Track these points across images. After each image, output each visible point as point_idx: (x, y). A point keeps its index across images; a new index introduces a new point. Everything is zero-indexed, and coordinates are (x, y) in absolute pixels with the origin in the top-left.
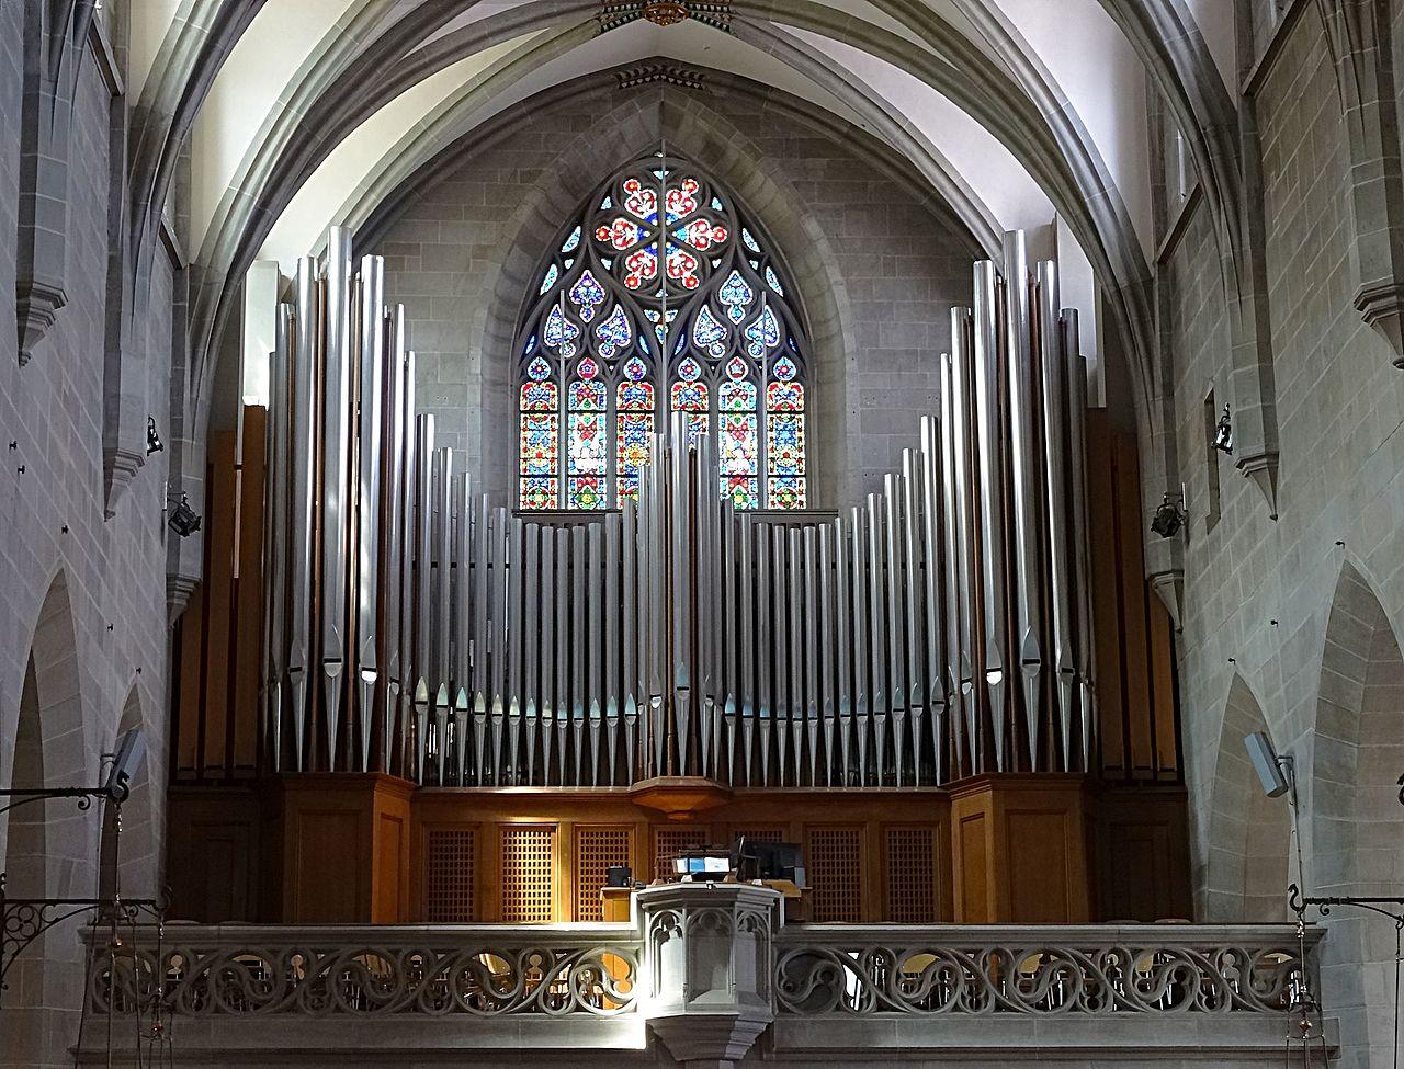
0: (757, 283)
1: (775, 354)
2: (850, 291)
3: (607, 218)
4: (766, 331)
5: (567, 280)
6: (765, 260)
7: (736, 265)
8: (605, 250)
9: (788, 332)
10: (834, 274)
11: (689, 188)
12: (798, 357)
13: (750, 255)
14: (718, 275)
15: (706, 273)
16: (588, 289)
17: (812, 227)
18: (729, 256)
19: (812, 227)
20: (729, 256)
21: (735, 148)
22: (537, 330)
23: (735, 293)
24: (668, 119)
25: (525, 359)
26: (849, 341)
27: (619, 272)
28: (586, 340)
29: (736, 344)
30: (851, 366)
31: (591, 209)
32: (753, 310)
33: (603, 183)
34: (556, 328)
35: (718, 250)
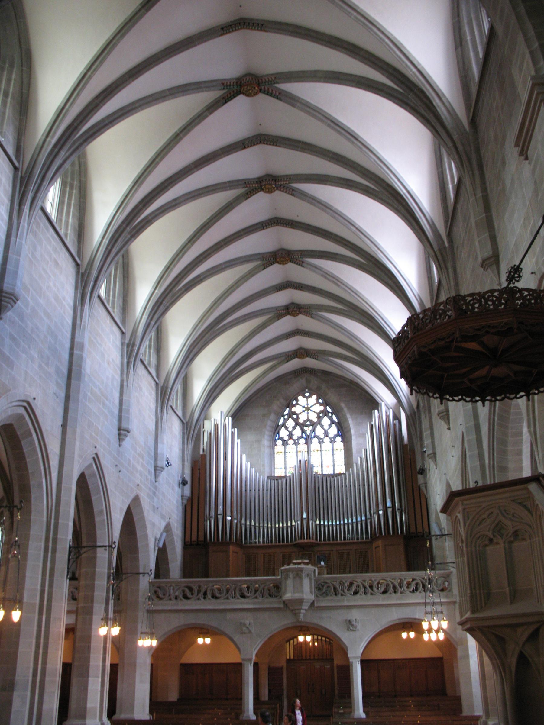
0: (331, 418)
1: (336, 436)
2: (352, 420)
3: (294, 406)
4: (333, 431)
5: (286, 421)
6: (333, 413)
7: (326, 415)
8: (294, 413)
9: (339, 430)
10: (348, 416)
11: (315, 397)
12: (342, 436)
13: (329, 412)
14: (321, 418)
15: (319, 418)
16: (290, 423)
17: (343, 405)
18: (325, 413)
19: (343, 405)
20: (325, 413)
21: (324, 386)
22: (278, 433)
23: (326, 421)
24: (308, 381)
25: (276, 440)
26: (353, 432)
27: (298, 418)
28: (291, 435)
29: (326, 434)
30: (353, 438)
31: (291, 403)
32: (330, 426)
33: (293, 397)
34: (284, 433)
35: (321, 412)
